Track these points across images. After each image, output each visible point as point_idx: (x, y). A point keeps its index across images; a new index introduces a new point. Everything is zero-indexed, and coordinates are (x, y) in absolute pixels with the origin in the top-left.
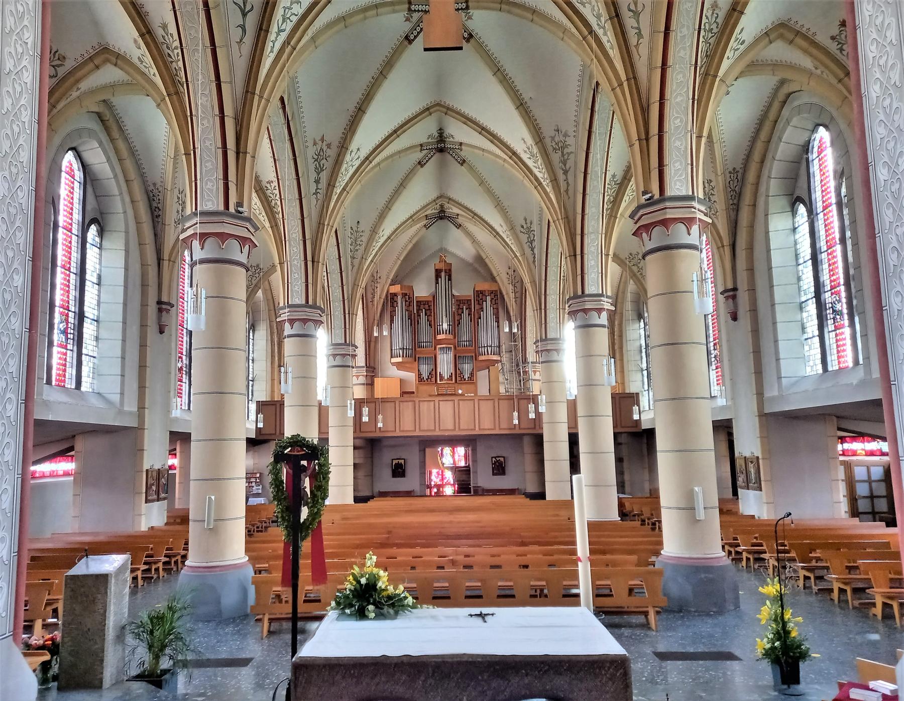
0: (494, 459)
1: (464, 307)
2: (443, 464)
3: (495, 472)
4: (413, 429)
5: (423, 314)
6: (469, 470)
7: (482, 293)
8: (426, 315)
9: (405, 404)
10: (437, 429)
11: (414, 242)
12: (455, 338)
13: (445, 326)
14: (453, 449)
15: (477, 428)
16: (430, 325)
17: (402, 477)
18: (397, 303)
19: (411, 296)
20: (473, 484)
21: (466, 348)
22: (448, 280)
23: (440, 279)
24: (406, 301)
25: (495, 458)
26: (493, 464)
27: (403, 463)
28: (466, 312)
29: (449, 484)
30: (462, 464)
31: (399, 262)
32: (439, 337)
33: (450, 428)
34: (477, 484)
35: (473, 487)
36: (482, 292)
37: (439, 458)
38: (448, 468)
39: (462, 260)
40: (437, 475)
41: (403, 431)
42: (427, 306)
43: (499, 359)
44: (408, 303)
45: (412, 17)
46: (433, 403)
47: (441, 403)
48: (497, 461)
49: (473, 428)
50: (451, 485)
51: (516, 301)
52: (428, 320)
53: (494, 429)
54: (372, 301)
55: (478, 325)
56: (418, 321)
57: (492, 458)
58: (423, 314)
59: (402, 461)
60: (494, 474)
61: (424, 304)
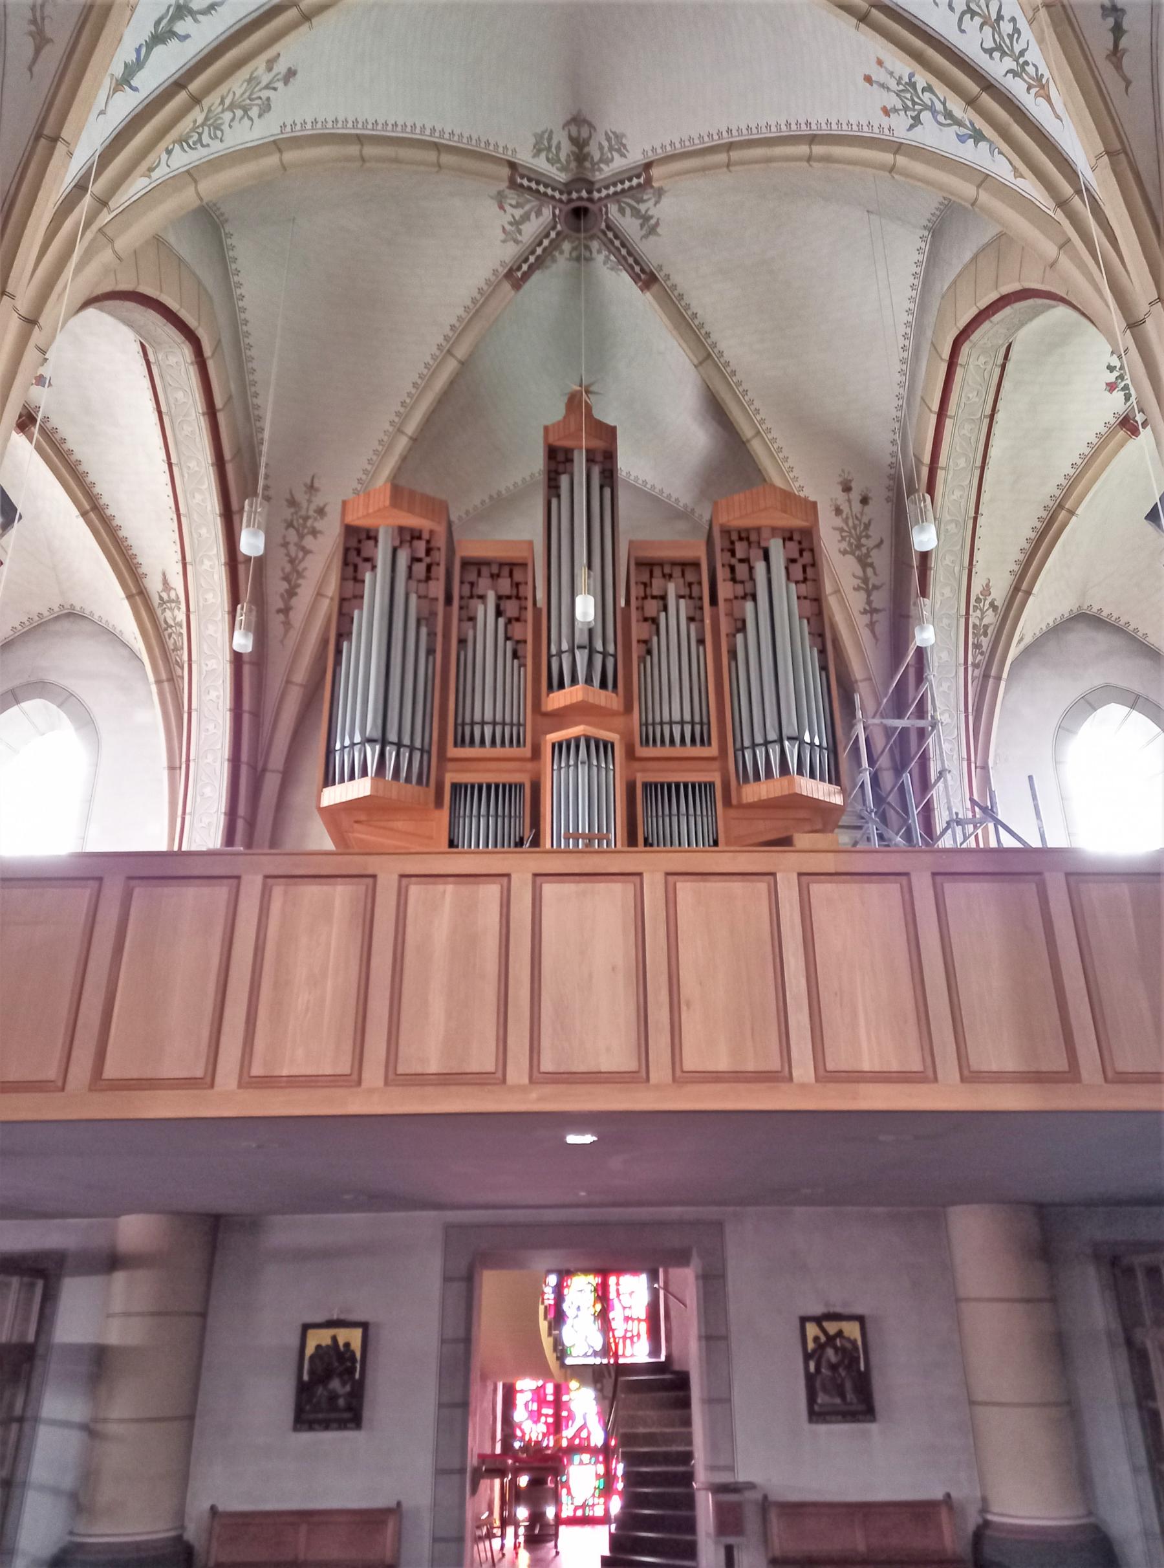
0: (812, 1330)
1: (672, 589)
2: (561, 1351)
3: (821, 1398)
4: (344, 1066)
5: (485, 612)
6: (681, 1382)
7: (748, 539)
8: (499, 613)
9: (312, 891)
10: (517, 1073)
11: (461, 352)
12: (628, 709)
13: (586, 608)
14: (604, 1286)
15: (804, 1070)
16: (515, 655)
17: (342, 1425)
18: (374, 568)
19: (440, 542)
20: (712, 1468)
21: (678, 751)
22: (602, 487)
23: (564, 480)
24: (415, 560)
25: (818, 1320)
26: (807, 1357)
27: (356, 1346)
28: (678, 610)
29: (584, 1448)
30: (638, 1353)
31: (402, 443)
32: (557, 700)
33: (607, 1064)
34: (731, 1468)
35: (719, 1489)
36: (744, 536)
37: (543, 1325)
38: (580, 1372)
39: (654, 500)
40: (535, 1407)
41: (268, 1082)
42: (505, 586)
43: (838, 800)
44: (420, 569)
45: (520, 232)
46: (491, 892)
47: (549, 889)
48: (831, 1339)
49: (774, 1063)
50: (594, 1451)
51: (871, 626)
52: (507, 638)
53: (927, 1076)
54: (286, 610)
55: (733, 654)
56: (462, 642)
57: (804, 1320)
58: (485, 612)
59: (354, 1337)
60: (816, 1415)
61: (494, 577)
